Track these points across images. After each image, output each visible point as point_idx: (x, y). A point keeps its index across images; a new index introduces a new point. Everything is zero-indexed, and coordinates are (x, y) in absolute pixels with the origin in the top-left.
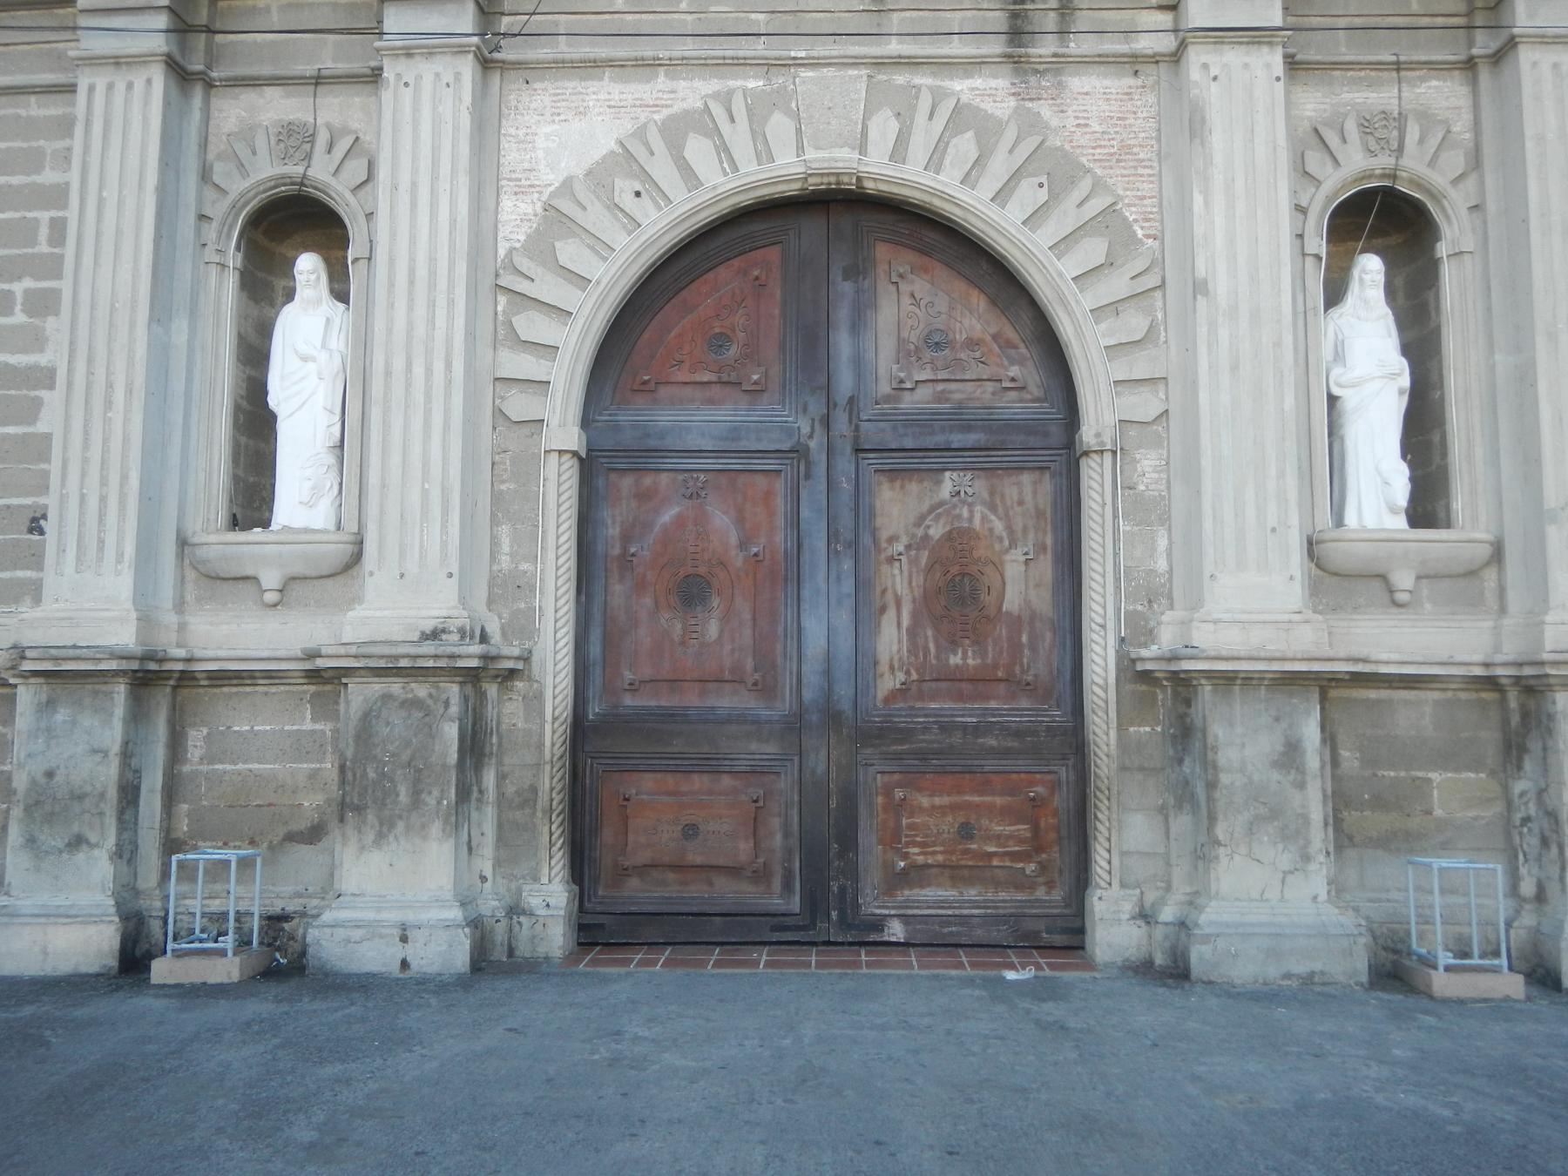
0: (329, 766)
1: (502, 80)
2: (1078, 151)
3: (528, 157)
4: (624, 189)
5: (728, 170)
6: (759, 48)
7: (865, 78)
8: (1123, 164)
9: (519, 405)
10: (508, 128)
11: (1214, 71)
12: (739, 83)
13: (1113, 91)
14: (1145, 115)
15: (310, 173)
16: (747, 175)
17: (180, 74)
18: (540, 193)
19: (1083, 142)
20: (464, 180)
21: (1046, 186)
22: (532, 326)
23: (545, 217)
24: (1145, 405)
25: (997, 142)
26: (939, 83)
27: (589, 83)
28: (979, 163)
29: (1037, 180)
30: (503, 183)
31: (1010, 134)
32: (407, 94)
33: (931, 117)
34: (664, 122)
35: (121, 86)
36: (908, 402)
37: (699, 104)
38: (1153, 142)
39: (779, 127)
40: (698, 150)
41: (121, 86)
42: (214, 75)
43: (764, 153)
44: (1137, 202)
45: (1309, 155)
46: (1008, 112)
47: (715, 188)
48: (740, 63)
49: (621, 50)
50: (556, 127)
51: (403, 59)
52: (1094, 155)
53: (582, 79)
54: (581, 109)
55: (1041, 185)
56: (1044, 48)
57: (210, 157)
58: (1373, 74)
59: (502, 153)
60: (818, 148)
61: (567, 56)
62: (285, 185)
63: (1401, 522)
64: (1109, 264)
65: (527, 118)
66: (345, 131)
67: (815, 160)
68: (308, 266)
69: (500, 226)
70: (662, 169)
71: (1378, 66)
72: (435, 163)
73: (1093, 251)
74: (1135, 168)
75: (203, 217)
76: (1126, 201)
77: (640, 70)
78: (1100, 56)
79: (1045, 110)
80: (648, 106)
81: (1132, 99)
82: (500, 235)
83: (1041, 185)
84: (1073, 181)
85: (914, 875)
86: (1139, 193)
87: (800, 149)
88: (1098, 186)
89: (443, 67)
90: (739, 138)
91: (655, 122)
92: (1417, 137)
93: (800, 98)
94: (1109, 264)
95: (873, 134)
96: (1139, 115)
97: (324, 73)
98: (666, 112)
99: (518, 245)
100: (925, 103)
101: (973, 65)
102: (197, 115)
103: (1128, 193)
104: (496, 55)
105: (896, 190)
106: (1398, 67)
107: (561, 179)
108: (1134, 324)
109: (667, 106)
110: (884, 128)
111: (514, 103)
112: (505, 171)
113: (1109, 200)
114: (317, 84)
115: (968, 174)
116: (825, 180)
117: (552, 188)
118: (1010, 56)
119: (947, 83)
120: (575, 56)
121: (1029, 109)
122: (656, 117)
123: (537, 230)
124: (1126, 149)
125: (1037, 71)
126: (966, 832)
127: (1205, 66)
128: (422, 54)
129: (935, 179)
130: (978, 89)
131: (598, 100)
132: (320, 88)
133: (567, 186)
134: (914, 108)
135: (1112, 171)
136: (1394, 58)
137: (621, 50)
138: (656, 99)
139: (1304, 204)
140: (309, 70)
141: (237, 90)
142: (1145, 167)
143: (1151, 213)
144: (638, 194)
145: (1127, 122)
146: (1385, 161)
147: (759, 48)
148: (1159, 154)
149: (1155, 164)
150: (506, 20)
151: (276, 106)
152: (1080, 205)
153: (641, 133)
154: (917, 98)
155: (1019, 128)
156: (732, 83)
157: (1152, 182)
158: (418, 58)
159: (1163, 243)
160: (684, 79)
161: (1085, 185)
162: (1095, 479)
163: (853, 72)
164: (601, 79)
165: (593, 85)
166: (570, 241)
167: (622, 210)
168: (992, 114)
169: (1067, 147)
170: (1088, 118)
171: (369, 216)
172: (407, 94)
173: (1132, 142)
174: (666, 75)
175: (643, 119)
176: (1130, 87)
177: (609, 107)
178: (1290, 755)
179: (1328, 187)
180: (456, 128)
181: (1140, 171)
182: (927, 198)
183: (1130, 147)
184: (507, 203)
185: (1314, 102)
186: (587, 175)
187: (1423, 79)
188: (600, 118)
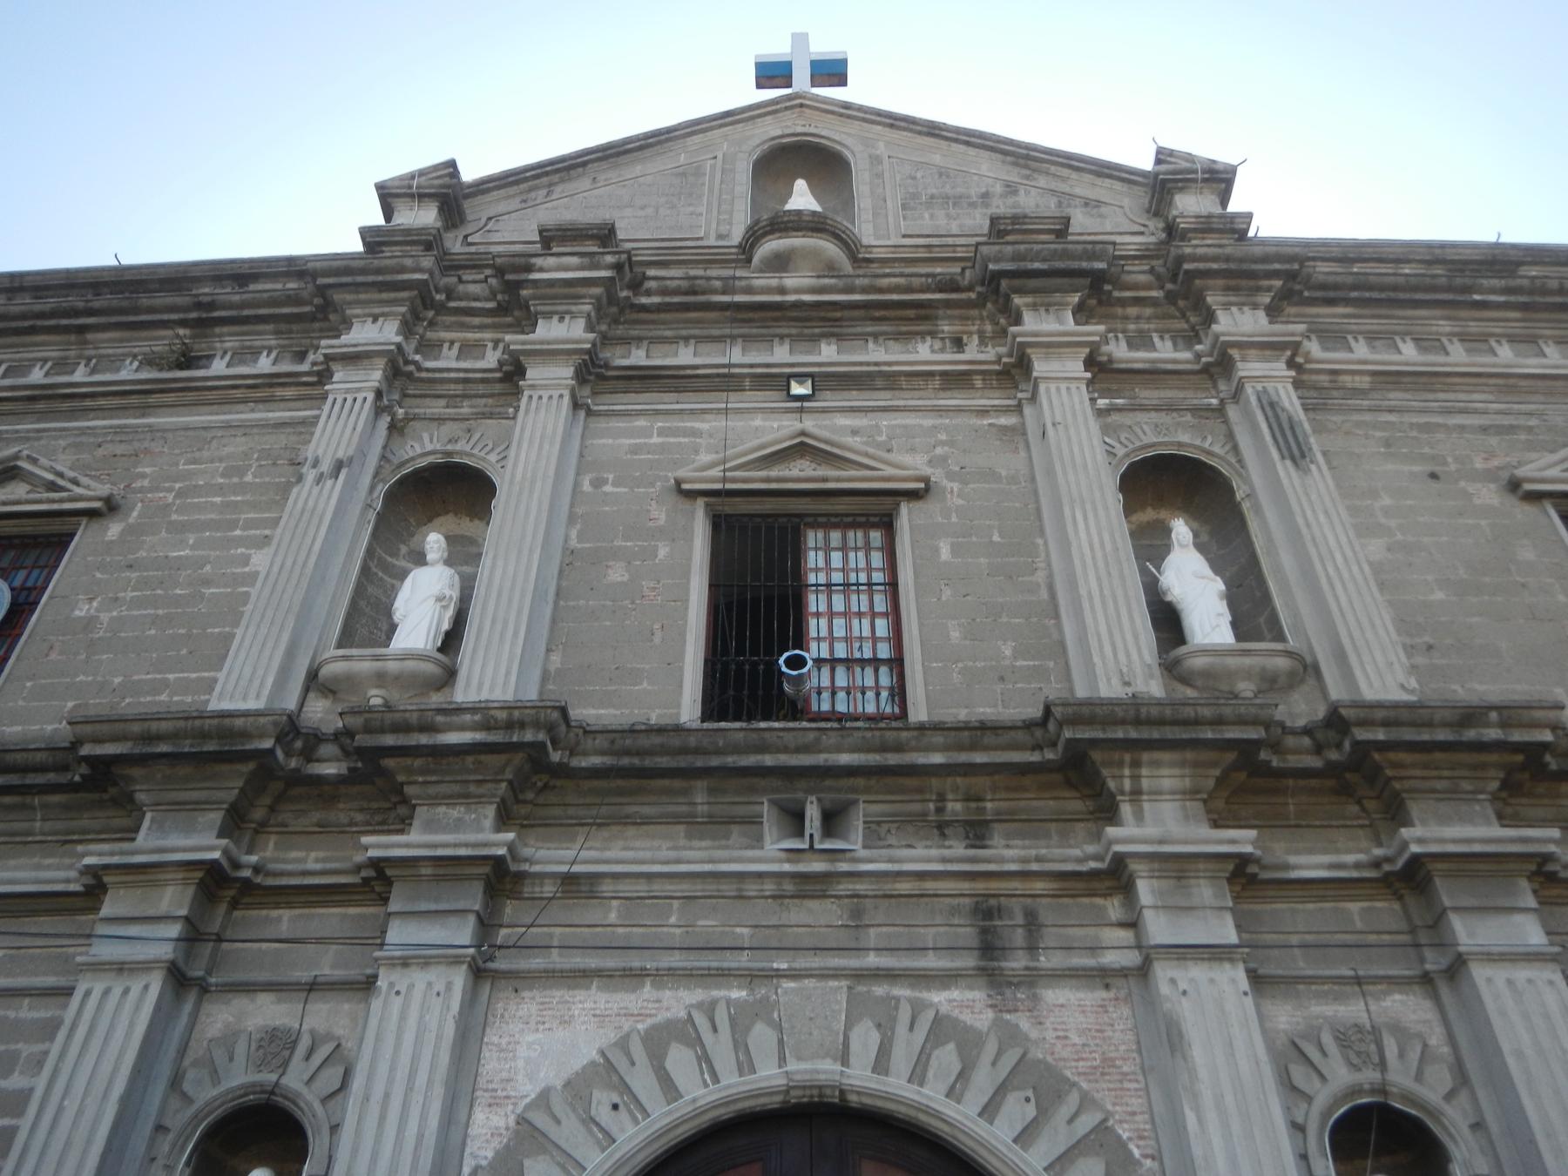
1: (491, 989)
2: (1061, 1064)
3: (507, 1066)
4: (601, 1099)
5: (709, 1081)
6: (743, 960)
7: (845, 989)
8: (1107, 1077)
10: (491, 1037)
11: (1183, 985)
12: (722, 993)
13: (1088, 1003)
14: (1122, 1027)
15: (284, 1081)
16: (729, 1086)
17: (179, 979)
18: (515, 1104)
19: (1065, 1054)
20: (439, 1091)
21: (1033, 1100)
23: (517, 1132)
25: (979, 1053)
26: (917, 994)
27: (576, 992)
28: (963, 1075)
29: (1022, 1094)
30: (478, 1093)
31: (991, 1048)
32: (397, 1003)
33: (911, 1028)
34: (647, 1031)
35: (117, 991)
37: (683, 1014)
38: (1135, 1055)
39: (761, 1036)
40: (679, 1060)
41: (117, 991)
42: (213, 980)
43: (746, 1065)
44: (1128, 1118)
45: (1293, 1068)
46: (987, 1024)
47: (694, 1100)
48: (722, 976)
49: (611, 962)
50: (540, 1036)
51: (399, 969)
52: (1077, 1068)
53: (570, 988)
54: (566, 1018)
55: (1028, 1100)
56: (1017, 963)
57: (186, 1062)
58: (1336, 987)
59: (482, 1062)
60: (799, 1059)
61: (558, 966)
62: (254, 1093)
65: (511, 1026)
66: (329, 1036)
67: (798, 1072)
69: (469, 1141)
70: (642, 1081)
71: (1339, 980)
72: (410, 1088)
74: (1121, 1081)
75: (160, 1128)
76: (1117, 1117)
77: (627, 980)
78: (1069, 969)
79: (1023, 1022)
80: (632, 1015)
81: (1107, 1012)
82: (468, 1151)
83: (1028, 1100)
84: (1059, 1096)
86: (1129, 1109)
87: (782, 1060)
88: (1086, 1102)
89: (436, 976)
91: (639, 1032)
92: (1396, 1050)
93: (782, 1009)
95: (855, 1046)
96: (1116, 1027)
97: (320, 980)
98: (649, 1021)
99: (484, 1163)
100: (904, 1014)
101: (946, 979)
102: (184, 1019)
103: (1118, 1108)
104: (490, 965)
105: (880, 1103)
106: (1358, 981)
107: (538, 1090)
109: (651, 1016)
110: (865, 1039)
111: (500, 1012)
112: (482, 1082)
113: (1099, 1117)
114: (310, 990)
115: (952, 1088)
116: (808, 1092)
117: (528, 1100)
118: (983, 969)
119: (925, 995)
120: (567, 966)
121: (1008, 1022)
122: (640, 1026)
123: (507, 1146)
124: (1108, 1062)
125: (1010, 984)
127: (1173, 981)
128: (418, 964)
129: (919, 1093)
130: (955, 1000)
131: (584, 1009)
132: (313, 995)
134: (894, 1020)
135: (1097, 1085)
136: (1351, 973)
137: (611, 962)
138: (642, 1008)
139: (1300, 1120)
140: (304, 975)
141: (230, 995)
142: (1130, 1081)
143: (1145, 1130)
144: (615, 1107)
145: (1106, 1034)
146: (1370, 1076)
147: (743, 960)
148: (1143, 1068)
149: (1141, 1078)
150: (503, 932)
151: (267, 1012)
152: (1071, 1121)
153: (623, 1044)
154: (897, 1008)
155: (1000, 1043)
156: (716, 993)
157: (1140, 1097)
158: (413, 968)
159: (1162, 1163)
160: (670, 989)
161: (1073, 1099)
163: (833, 983)
164: (588, 988)
165: (580, 994)
166: (541, 1158)
167: (597, 1124)
168: (971, 1026)
169: (1049, 1059)
170: (1066, 1030)
171: (335, 1129)
172: (397, 1003)
173: (1112, 1055)
174: (652, 986)
175: (626, 1028)
176: (1103, 1000)
177: (594, 1016)
179: (1321, 1101)
180: (439, 1037)
181: (1127, 1085)
182: (912, 1113)
183: (1113, 1060)
184: (479, 1115)
185: (1285, 1016)
186: (565, 1086)
187: (1386, 993)
188: (583, 1028)
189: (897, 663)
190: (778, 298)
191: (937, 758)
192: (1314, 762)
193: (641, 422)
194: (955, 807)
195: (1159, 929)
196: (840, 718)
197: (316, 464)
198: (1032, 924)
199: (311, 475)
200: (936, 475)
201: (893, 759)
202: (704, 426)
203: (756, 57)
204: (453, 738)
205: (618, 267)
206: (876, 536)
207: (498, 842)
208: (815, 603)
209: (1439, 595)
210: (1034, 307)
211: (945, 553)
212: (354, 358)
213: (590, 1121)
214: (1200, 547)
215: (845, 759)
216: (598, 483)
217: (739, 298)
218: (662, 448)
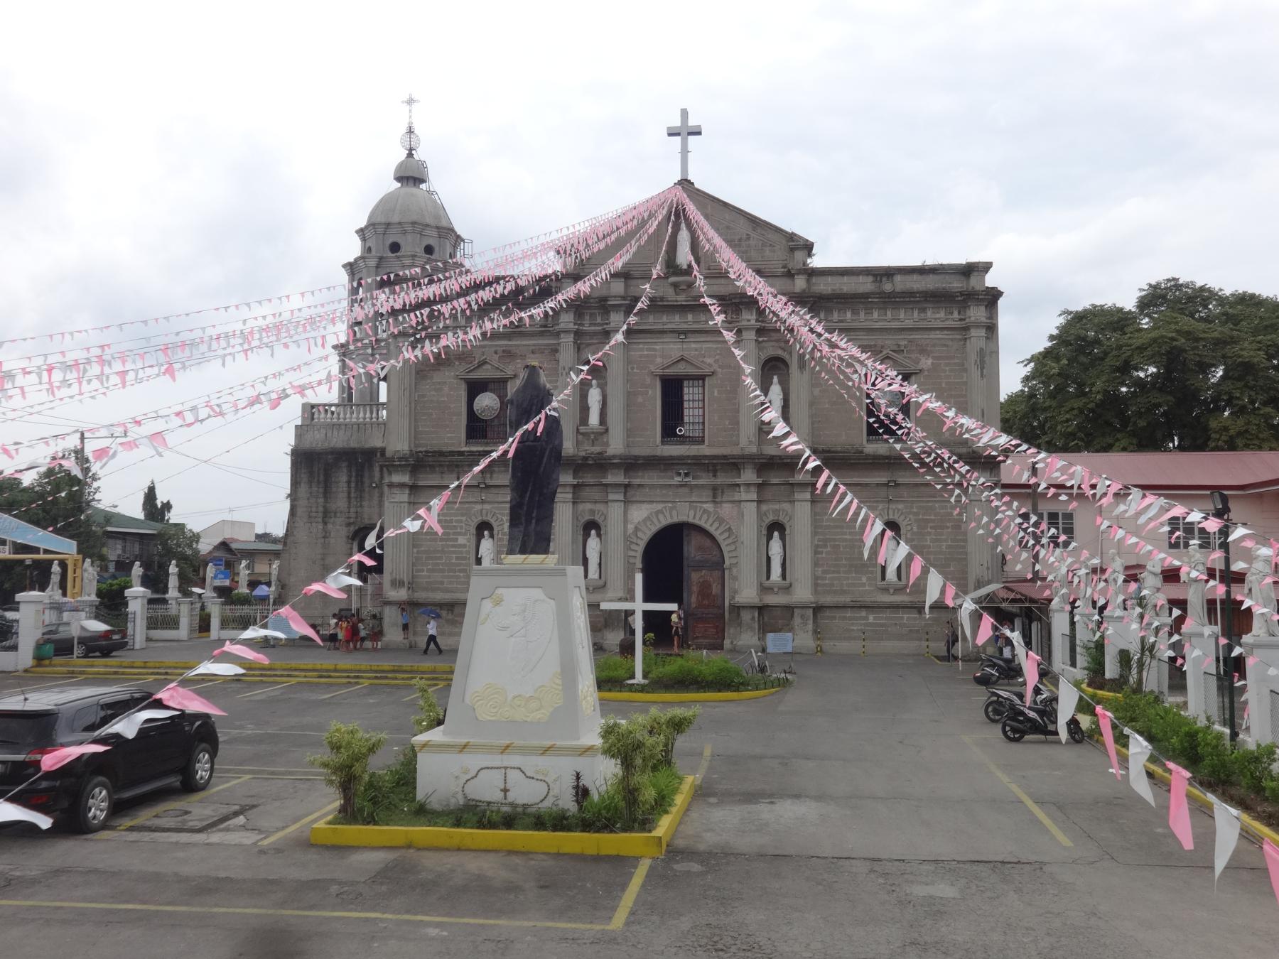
0: (602, 619)
4: (648, 523)
9: (632, 560)
17: (574, 503)
22: (633, 547)
24: (734, 561)
28: (708, 519)
36: (697, 558)
39: (674, 513)
40: (661, 517)
43: (672, 517)
63: (780, 579)
64: (729, 537)
68: (593, 532)
70: (655, 521)
73: (726, 535)
85: (697, 638)
88: (728, 523)
89: (619, 504)
90: (667, 514)
94: (729, 537)
101: (706, 502)
108: (733, 547)
110: (692, 513)
126: (706, 631)
133: (639, 523)
146: (776, 518)
151: (589, 506)
153: (651, 514)
162: (727, 572)
178: (753, 618)
185: (764, 507)
189: (703, 423)
190: (675, 303)
191: (707, 462)
192: (779, 461)
193: (641, 346)
194: (711, 468)
195: (744, 496)
196: (690, 437)
197: (564, 369)
198: (722, 492)
199: (564, 373)
200: (715, 367)
201: (698, 462)
202: (657, 347)
203: (668, 128)
204: (615, 461)
205: (631, 300)
206: (701, 382)
207: (626, 481)
208: (686, 405)
209: (827, 406)
210: (745, 308)
211: (716, 394)
212: (566, 332)
213: (647, 527)
214: (780, 383)
215: (689, 461)
216: (633, 368)
217: (665, 303)
218: (647, 356)
